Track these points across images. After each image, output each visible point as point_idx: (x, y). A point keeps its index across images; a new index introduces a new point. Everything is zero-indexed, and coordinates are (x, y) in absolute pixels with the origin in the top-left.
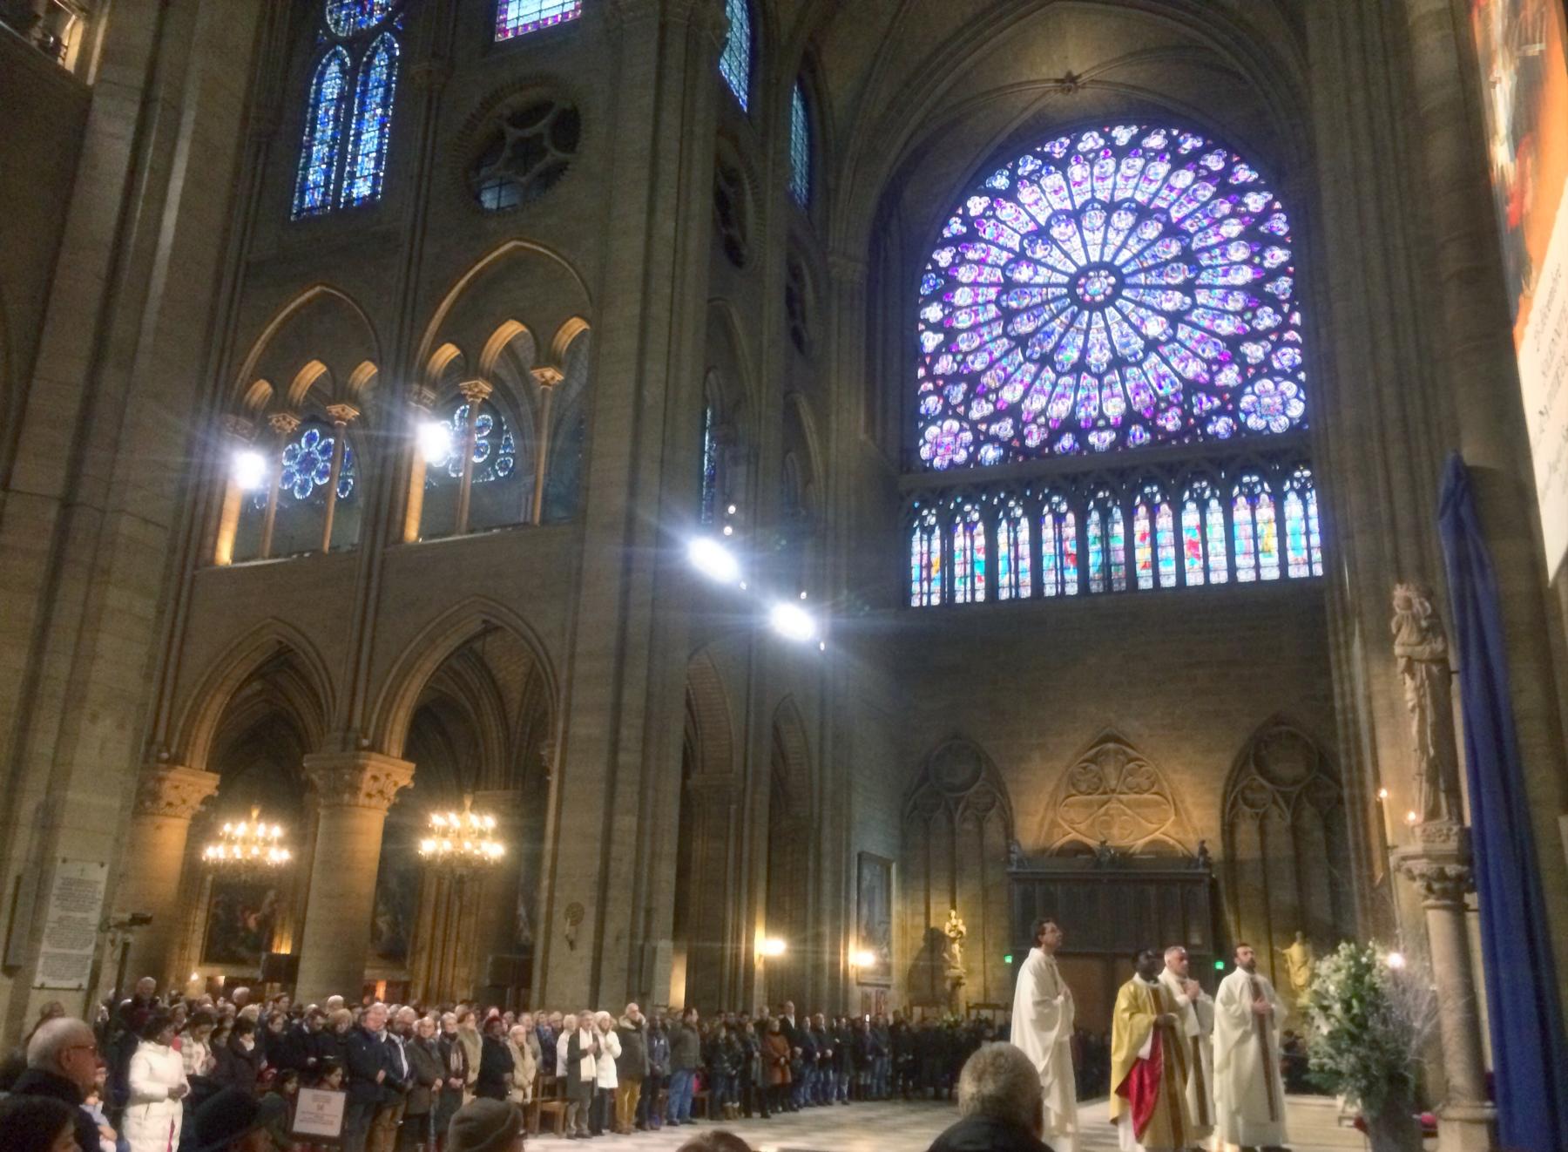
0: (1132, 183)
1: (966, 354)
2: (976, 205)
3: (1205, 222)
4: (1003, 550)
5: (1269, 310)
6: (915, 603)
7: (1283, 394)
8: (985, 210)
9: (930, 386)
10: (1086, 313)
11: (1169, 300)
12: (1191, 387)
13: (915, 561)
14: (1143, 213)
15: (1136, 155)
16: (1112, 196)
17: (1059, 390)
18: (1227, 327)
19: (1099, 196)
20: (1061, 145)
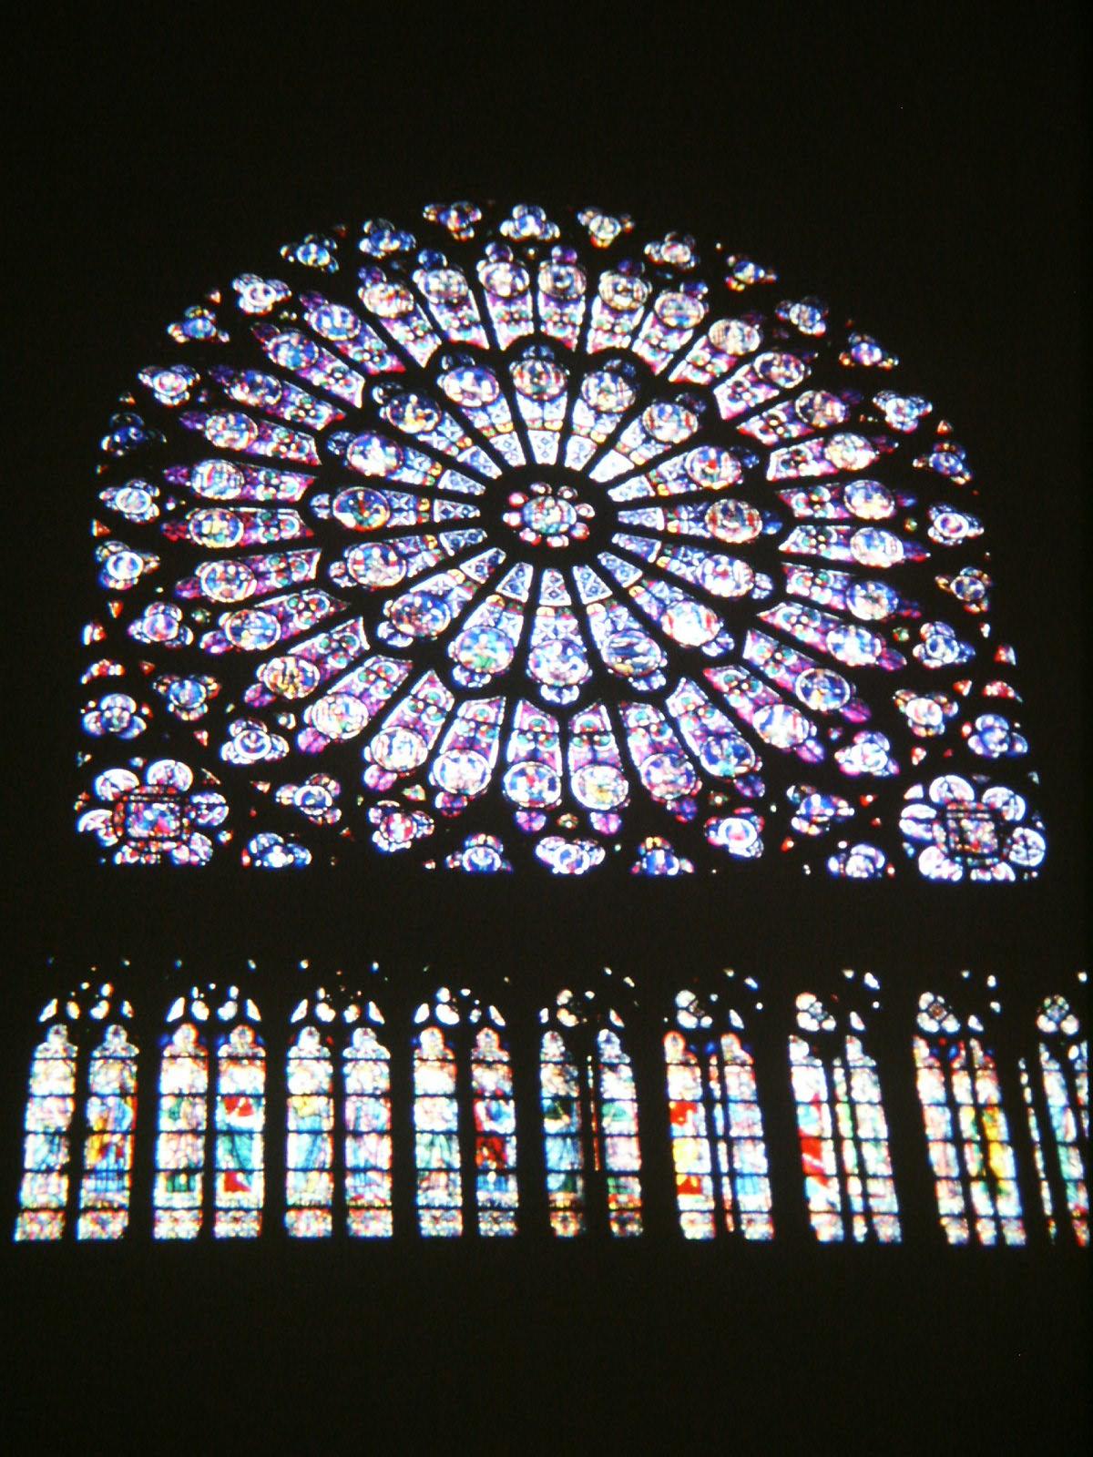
0: (627, 323)
1: (218, 609)
2: (256, 296)
3: (795, 430)
4: (308, 1111)
5: (949, 632)
6: (37, 1228)
7: (996, 815)
8: (278, 306)
9: (116, 670)
10: (529, 570)
11: (725, 574)
12: (781, 767)
13: (45, 1111)
14: (650, 387)
15: (631, 275)
16: (583, 339)
17: (460, 729)
18: (855, 650)
19: (551, 330)
20: (463, 216)
